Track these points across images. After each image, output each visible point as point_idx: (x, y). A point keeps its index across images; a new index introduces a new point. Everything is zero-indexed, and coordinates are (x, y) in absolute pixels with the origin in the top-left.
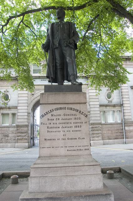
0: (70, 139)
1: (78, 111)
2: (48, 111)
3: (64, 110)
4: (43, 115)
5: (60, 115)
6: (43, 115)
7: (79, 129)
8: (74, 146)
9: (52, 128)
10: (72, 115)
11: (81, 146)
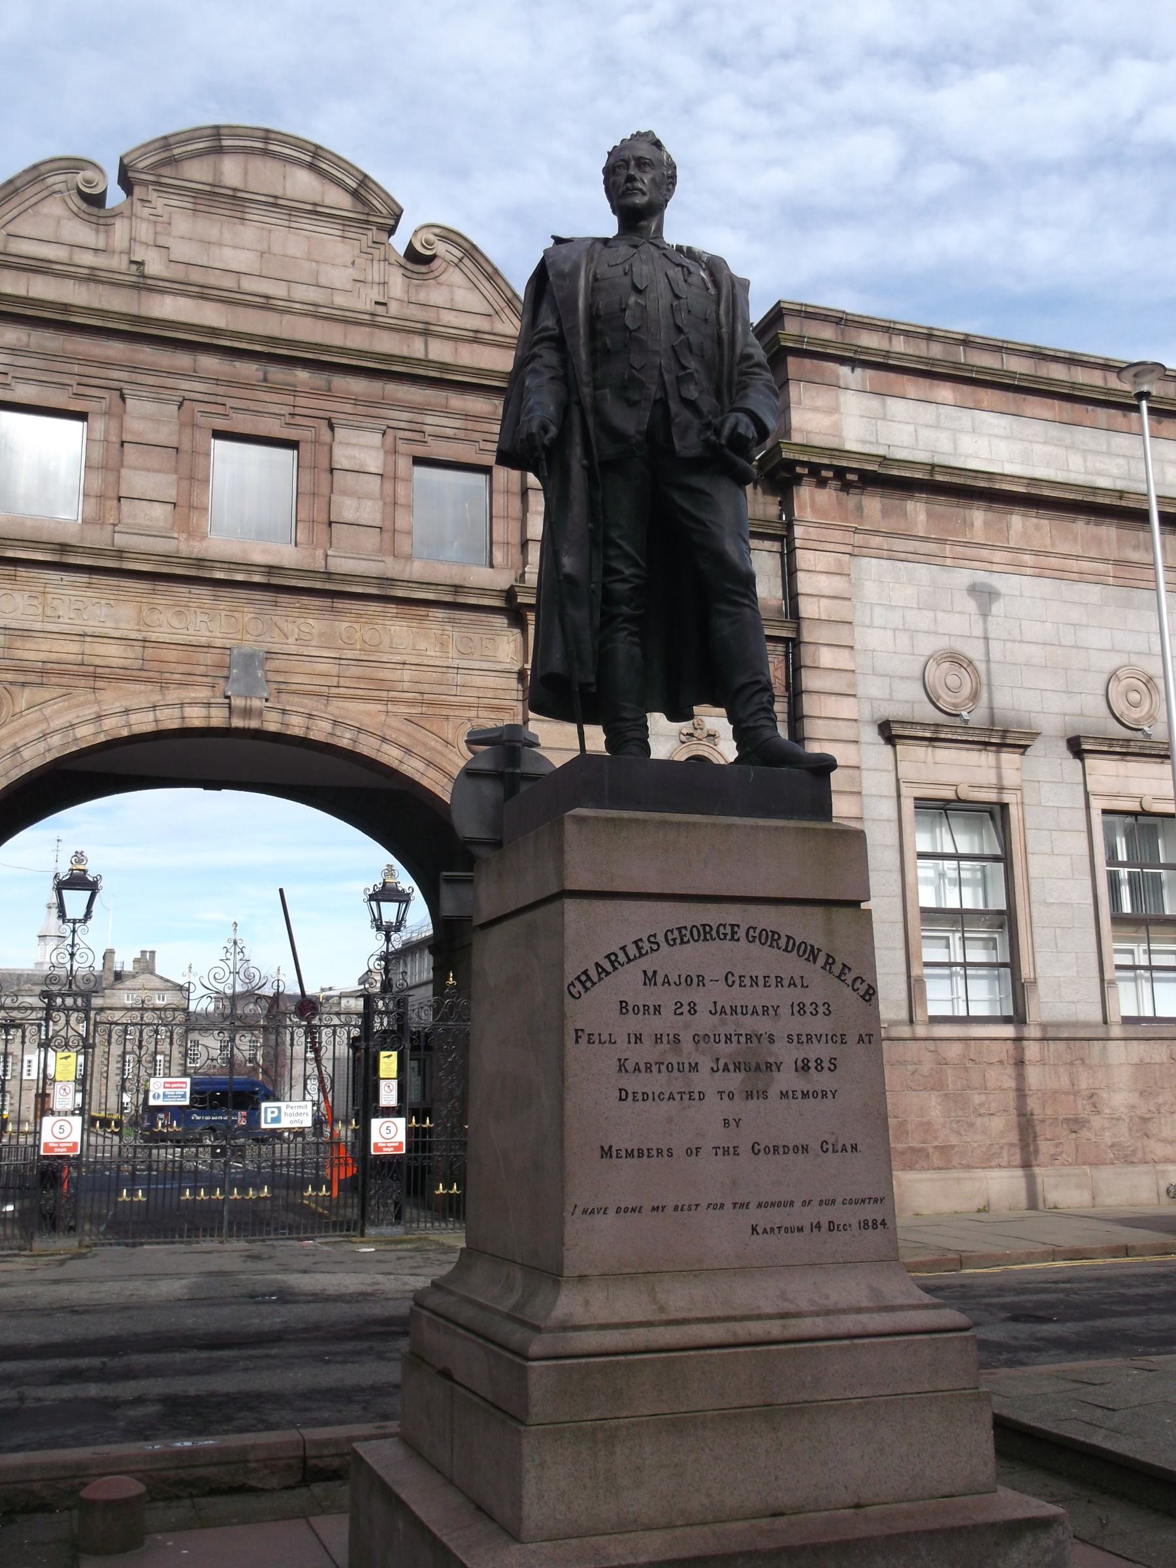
0: (767, 1150)
1: (813, 954)
2: (623, 948)
3: (727, 944)
4: (585, 972)
5: (701, 979)
6: (585, 972)
7: (822, 1080)
8: (792, 1203)
9: (649, 1068)
10: (779, 981)
11: (839, 1200)
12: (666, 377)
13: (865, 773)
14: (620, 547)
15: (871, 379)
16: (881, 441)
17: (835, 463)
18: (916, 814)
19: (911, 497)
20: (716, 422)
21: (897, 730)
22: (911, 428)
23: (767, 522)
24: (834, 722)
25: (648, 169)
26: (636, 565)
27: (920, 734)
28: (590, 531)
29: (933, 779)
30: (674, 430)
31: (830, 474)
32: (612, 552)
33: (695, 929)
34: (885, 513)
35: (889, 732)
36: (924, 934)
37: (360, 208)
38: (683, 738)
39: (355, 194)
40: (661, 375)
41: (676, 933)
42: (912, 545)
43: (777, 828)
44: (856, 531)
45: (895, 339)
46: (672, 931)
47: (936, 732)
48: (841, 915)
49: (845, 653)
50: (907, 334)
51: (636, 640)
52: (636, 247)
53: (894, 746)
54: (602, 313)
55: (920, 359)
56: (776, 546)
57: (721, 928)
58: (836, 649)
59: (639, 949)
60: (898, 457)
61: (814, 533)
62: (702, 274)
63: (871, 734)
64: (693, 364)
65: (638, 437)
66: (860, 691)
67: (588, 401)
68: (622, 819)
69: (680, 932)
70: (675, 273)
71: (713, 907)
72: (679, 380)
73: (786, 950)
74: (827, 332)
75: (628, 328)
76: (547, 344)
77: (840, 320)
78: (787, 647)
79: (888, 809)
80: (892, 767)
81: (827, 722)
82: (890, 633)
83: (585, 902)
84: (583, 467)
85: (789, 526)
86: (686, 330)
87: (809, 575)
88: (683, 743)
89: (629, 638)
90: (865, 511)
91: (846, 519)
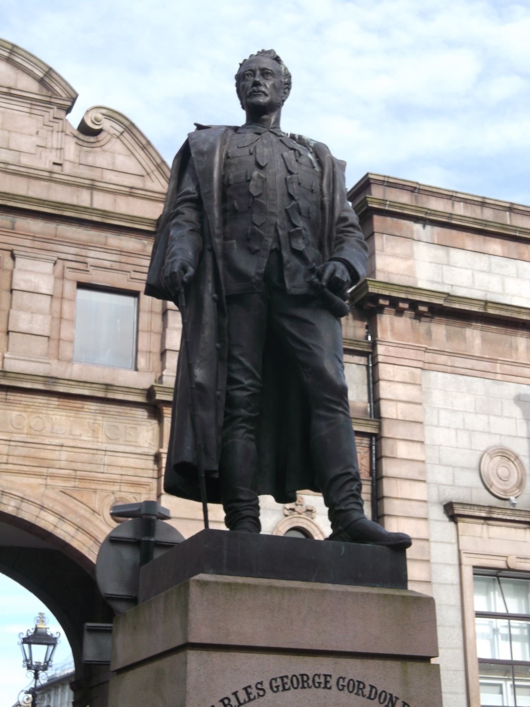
2: (235, 694)
3: (321, 692)
12: (281, 232)
13: (433, 545)
14: (240, 362)
15: (438, 234)
16: (446, 282)
17: (410, 297)
18: (475, 580)
19: (470, 326)
20: (319, 268)
21: (458, 510)
22: (469, 272)
23: (356, 342)
24: (408, 502)
25: (270, 77)
26: (254, 377)
27: (477, 514)
28: (218, 349)
29: (487, 551)
30: (286, 273)
31: (406, 306)
32: (234, 366)
33: (294, 678)
34: (449, 337)
35: (452, 512)
36: (481, 681)
37: (45, 92)
38: (287, 512)
39: (41, 81)
40: (276, 231)
41: (279, 681)
42: (470, 363)
43: (363, 594)
44: (426, 350)
45: (456, 204)
46: (275, 679)
47: (490, 512)
48: (414, 667)
49: (418, 446)
50: (465, 201)
51: (252, 436)
52: (259, 134)
53: (456, 523)
54: (231, 183)
55: (475, 220)
56: (363, 360)
57: (317, 678)
58: (410, 444)
59: (248, 694)
60: (459, 294)
61: (393, 351)
62: (310, 156)
63: (437, 513)
64: (301, 224)
65: (258, 278)
66: (429, 478)
67: (219, 249)
68: (236, 584)
69: (282, 680)
70: (289, 155)
71: (310, 660)
72: (291, 236)
73: (369, 698)
74: (404, 198)
75: (251, 194)
76: (189, 204)
77: (414, 189)
78: (371, 441)
79: (451, 575)
80: (454, 540)
81: (402, 502)
82: (453, 432)
83: (205, 654)
84: (214, 299)
85: (374, 345)
86: (296, 197)
87: (388, 384)
88: (286, 516)
89: (246, 435)
90: (434, 335)
91: (418, 341)
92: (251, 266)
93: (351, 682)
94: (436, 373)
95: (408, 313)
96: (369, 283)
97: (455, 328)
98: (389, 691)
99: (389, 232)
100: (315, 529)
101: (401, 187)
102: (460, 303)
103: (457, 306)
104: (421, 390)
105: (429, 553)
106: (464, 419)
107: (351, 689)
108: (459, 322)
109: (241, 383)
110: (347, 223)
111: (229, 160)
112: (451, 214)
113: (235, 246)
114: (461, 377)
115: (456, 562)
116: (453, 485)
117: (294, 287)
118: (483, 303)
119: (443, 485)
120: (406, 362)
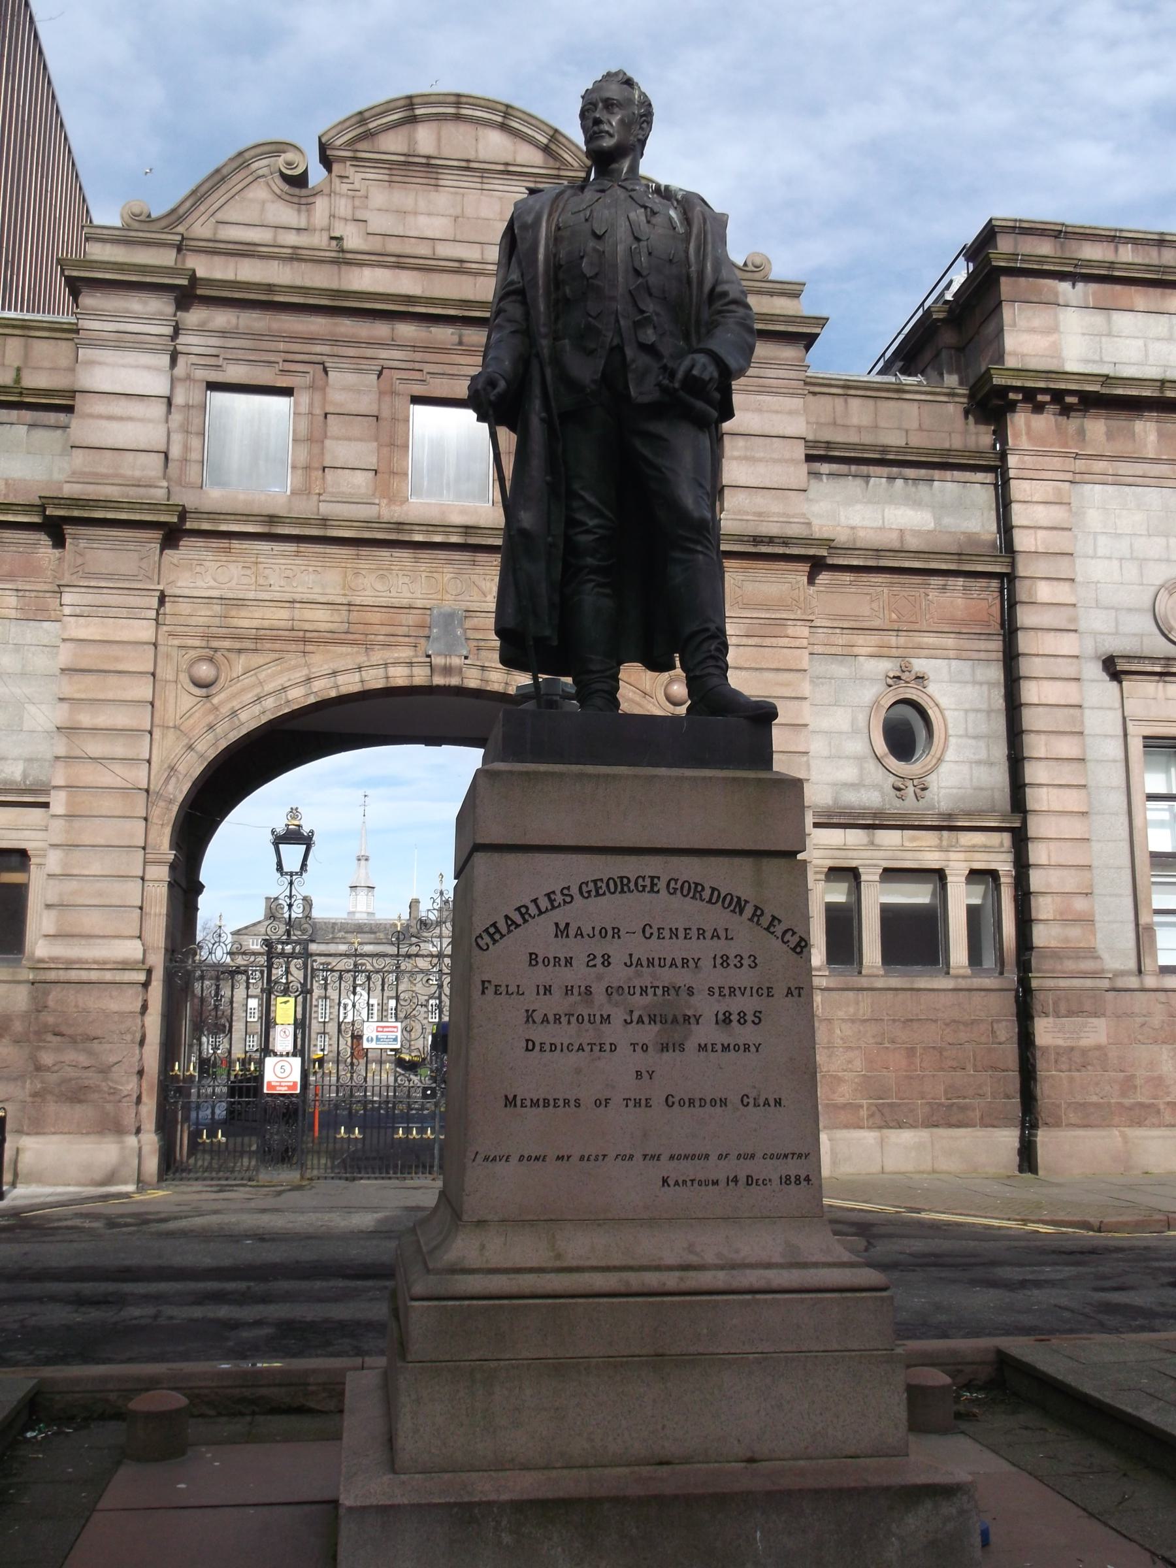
0: (681, 1102)
1: (739, 906)
3: (646, 896)
4: (494, 925)
5: (616, 932)
6: (494, 925)
7: (744, 1034)
8: (707, 1156)
9: (557, 1019)
10: (701, 933)
11: (759, 1155)
12: (622, 322)
13: (1087, 712)
14: (582, 498)
15: (1094, 294)
16: (1106, 359)
17: (1052, 386)
18: (1145, 753)
19: (1140, 417)
20: (670, 365)
21: (1122, 666)
22: (1140, 343)
23: (979, 453)
24: (1052, 659)
25: (616, 110)
26: (601, 515)
27: (1149, 669)
28: (548, 484)
29: (1163, 717)
30: (630, 376)
31: (1047, 398)
32: (576, 504)
33: (611, 882)
34: (1110, 436)
35: (1113, 668)
36: (1153, 879)
37: (551, 163)
38: (890, 681)
39: (546, 149)
40: (617, 321)
41: (591, 885)
42: (1140, 468)
43: (704, 778)
44: (1077, 456)
45: (1121, 248)
46: (587, 884)
47: (1168, 666)
48: (771, 866)
49: (1066, 586)
50: (1134, 241)
51: (607, 591)
52: (603, 191)
53: (1120, 682)
54: (562, 262)
55: (1148, 267)
56: (989, 477)
57: (640, 881)
58: (1055, 583)
59: (551, 901)
60: (1125, 375)
61: (1029, 461)
62: (672, 213)
63: (1095, 671)
64: (650, 307)
65: (593, 387)
66: (1083, 625)
67: (546, 352)
68: (536, 773)
69: (596, 884)
70: (638, 215)
71: (632, 859)
72: (637, 325)
73: (710, 901)
74: (1045, 248)
75: (585, 275)
76: (513, 298)
77: (1059, 233)
78: (1002, 583)
79: (1114, 749)
80: (1118, 705)
81: (1045, 659)
82: (1116, 563)
83: (496, 856)
84: (542, 420)
85: (1003, 456)
86: (644, 273)
87: (1024, 506)
88: (890, 686)
89: (596, 590)
90: (1088, 434)
91: (1065, 445)
92: (585, 370)
93: (686, 885)
94: (1091, 486)
95: (1051, 408)
96: (992, 372)
97: (1119, 422)
98: (735, 894)
99: (1022, 299)
100: (928, 700)
101: (1039, 232)
102: (1124, 386)
103: (1120, 391)
104: (1070, 510)
105: (1082, 723)
106: (1131, 545)
107: (685, 892)
108: (1123, 414)
109: (583, 524)
110: (727, 300)
111: (560, 233)
112: (1112, 263)
113: (568, 348)
114: (1127, 489)
115: (1120, 732)
116: (1117, 633)
117: (641, 394)
118: (1158, 384)
119: (1101, 634)
120: (1048, 475)
